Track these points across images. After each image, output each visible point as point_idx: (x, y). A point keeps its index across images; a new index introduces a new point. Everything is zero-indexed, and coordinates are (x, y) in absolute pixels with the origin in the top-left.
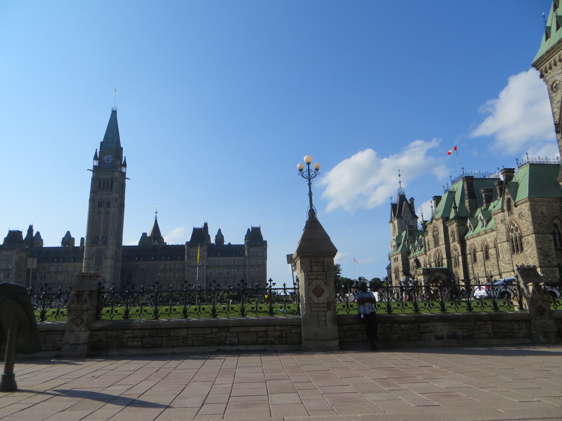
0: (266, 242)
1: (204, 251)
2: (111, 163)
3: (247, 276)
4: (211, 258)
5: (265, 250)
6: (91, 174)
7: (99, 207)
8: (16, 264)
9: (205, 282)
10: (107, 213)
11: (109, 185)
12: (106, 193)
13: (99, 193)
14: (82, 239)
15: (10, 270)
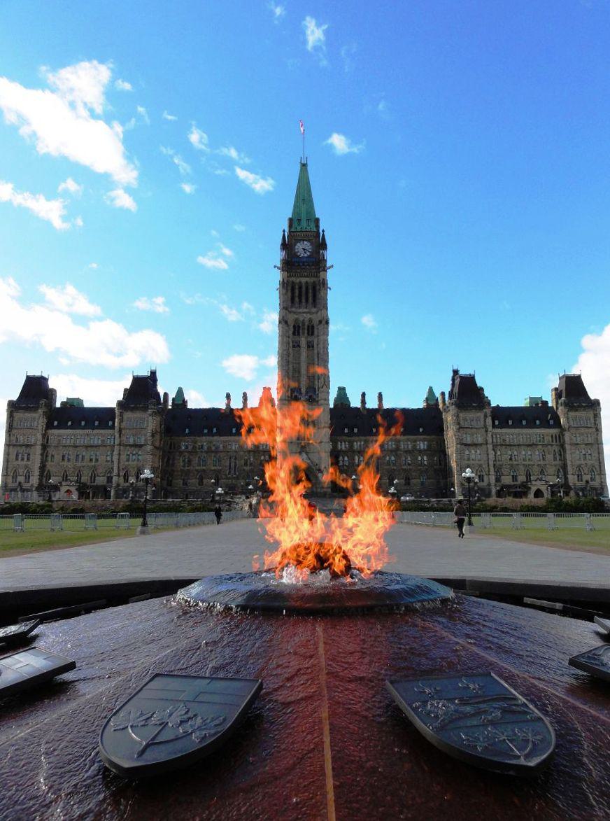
0: (596, 404)
1: (486, 416)
2: (308, 257)
3: (569, 463)
4: (499, 430)
5: (597, 416)
6: (276, 277)
7: (294, 334)
8: (153, 436)
9: (492, 472)
10: (310, 346)
11: (310, 295)
12: (305, 310)
13: (293, 309)
14: (245, 395)
15: (140, 446)
